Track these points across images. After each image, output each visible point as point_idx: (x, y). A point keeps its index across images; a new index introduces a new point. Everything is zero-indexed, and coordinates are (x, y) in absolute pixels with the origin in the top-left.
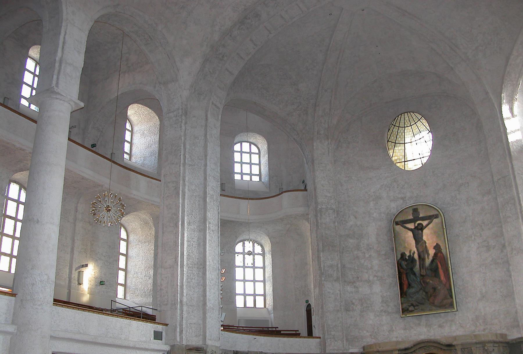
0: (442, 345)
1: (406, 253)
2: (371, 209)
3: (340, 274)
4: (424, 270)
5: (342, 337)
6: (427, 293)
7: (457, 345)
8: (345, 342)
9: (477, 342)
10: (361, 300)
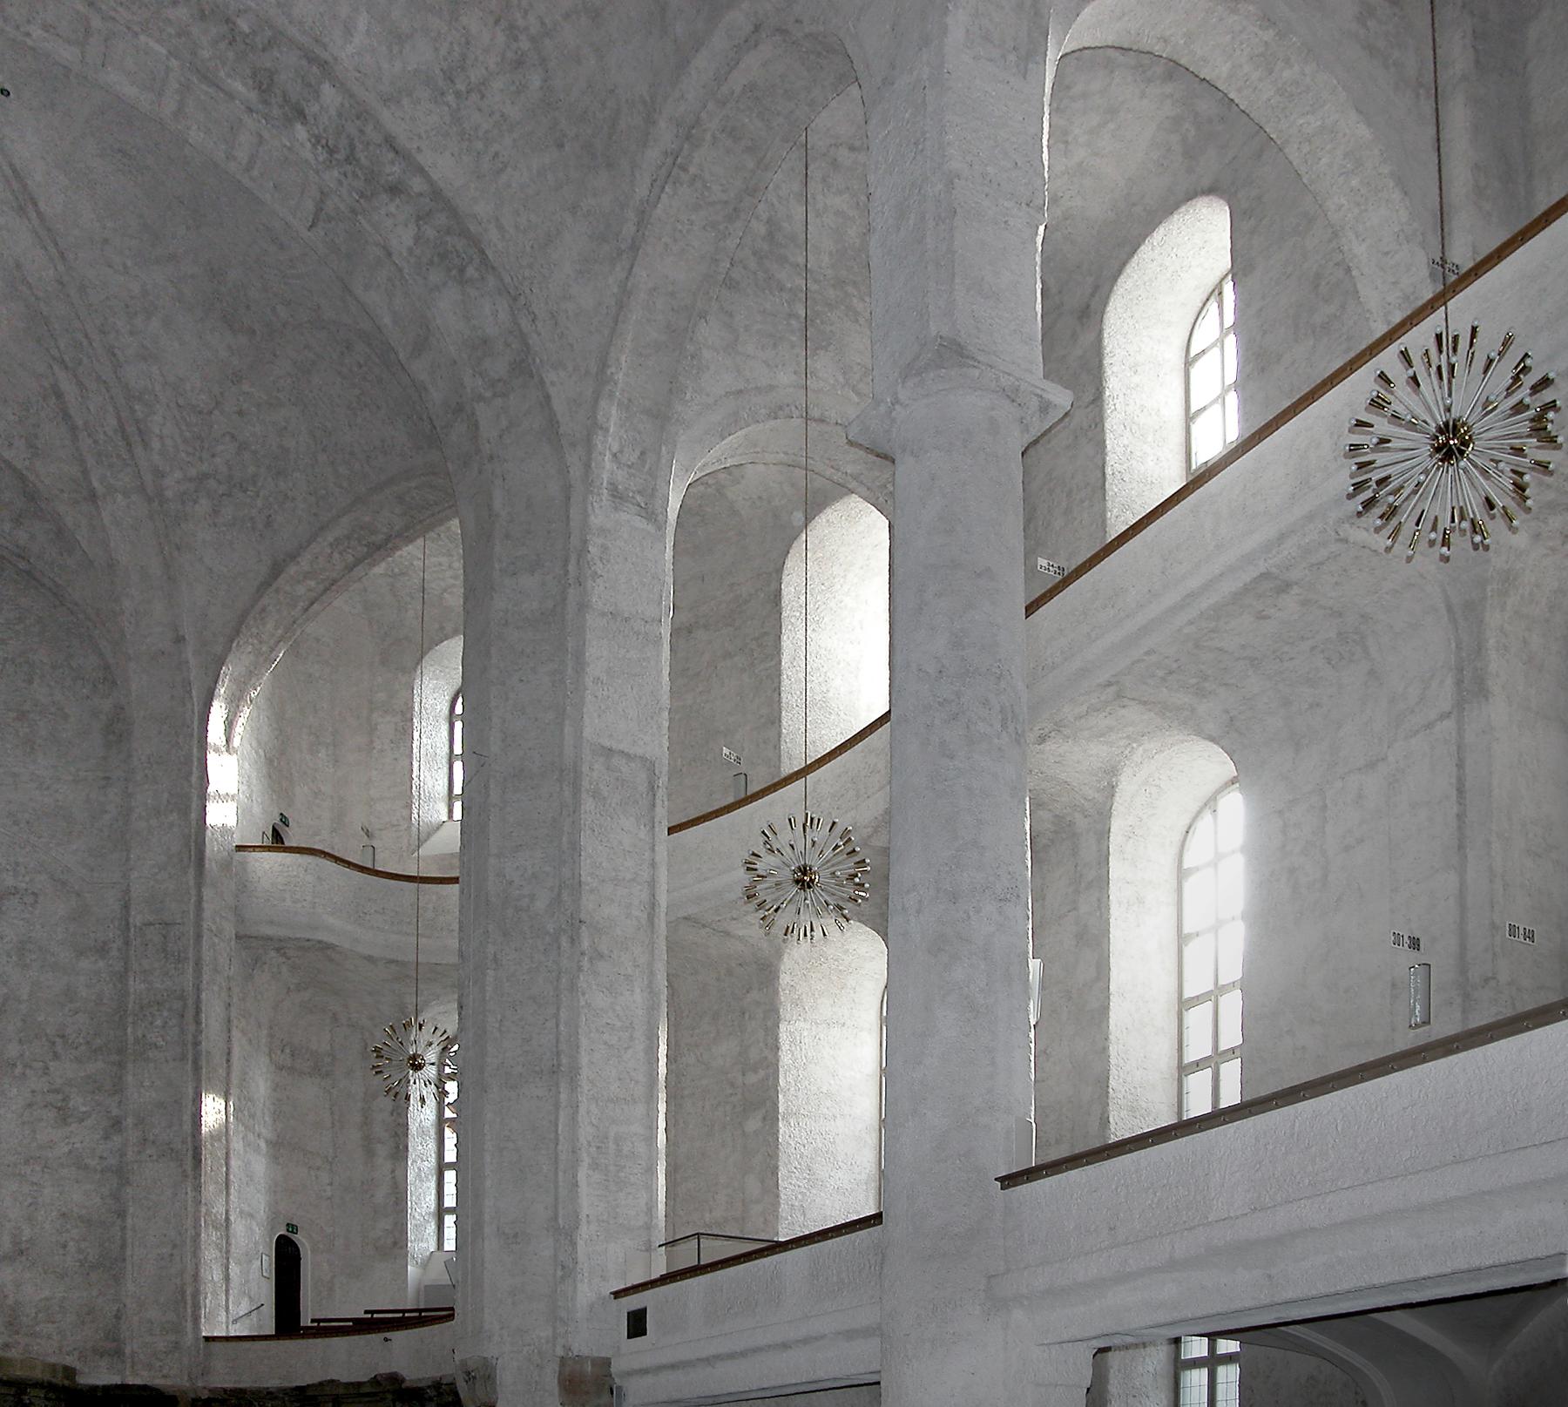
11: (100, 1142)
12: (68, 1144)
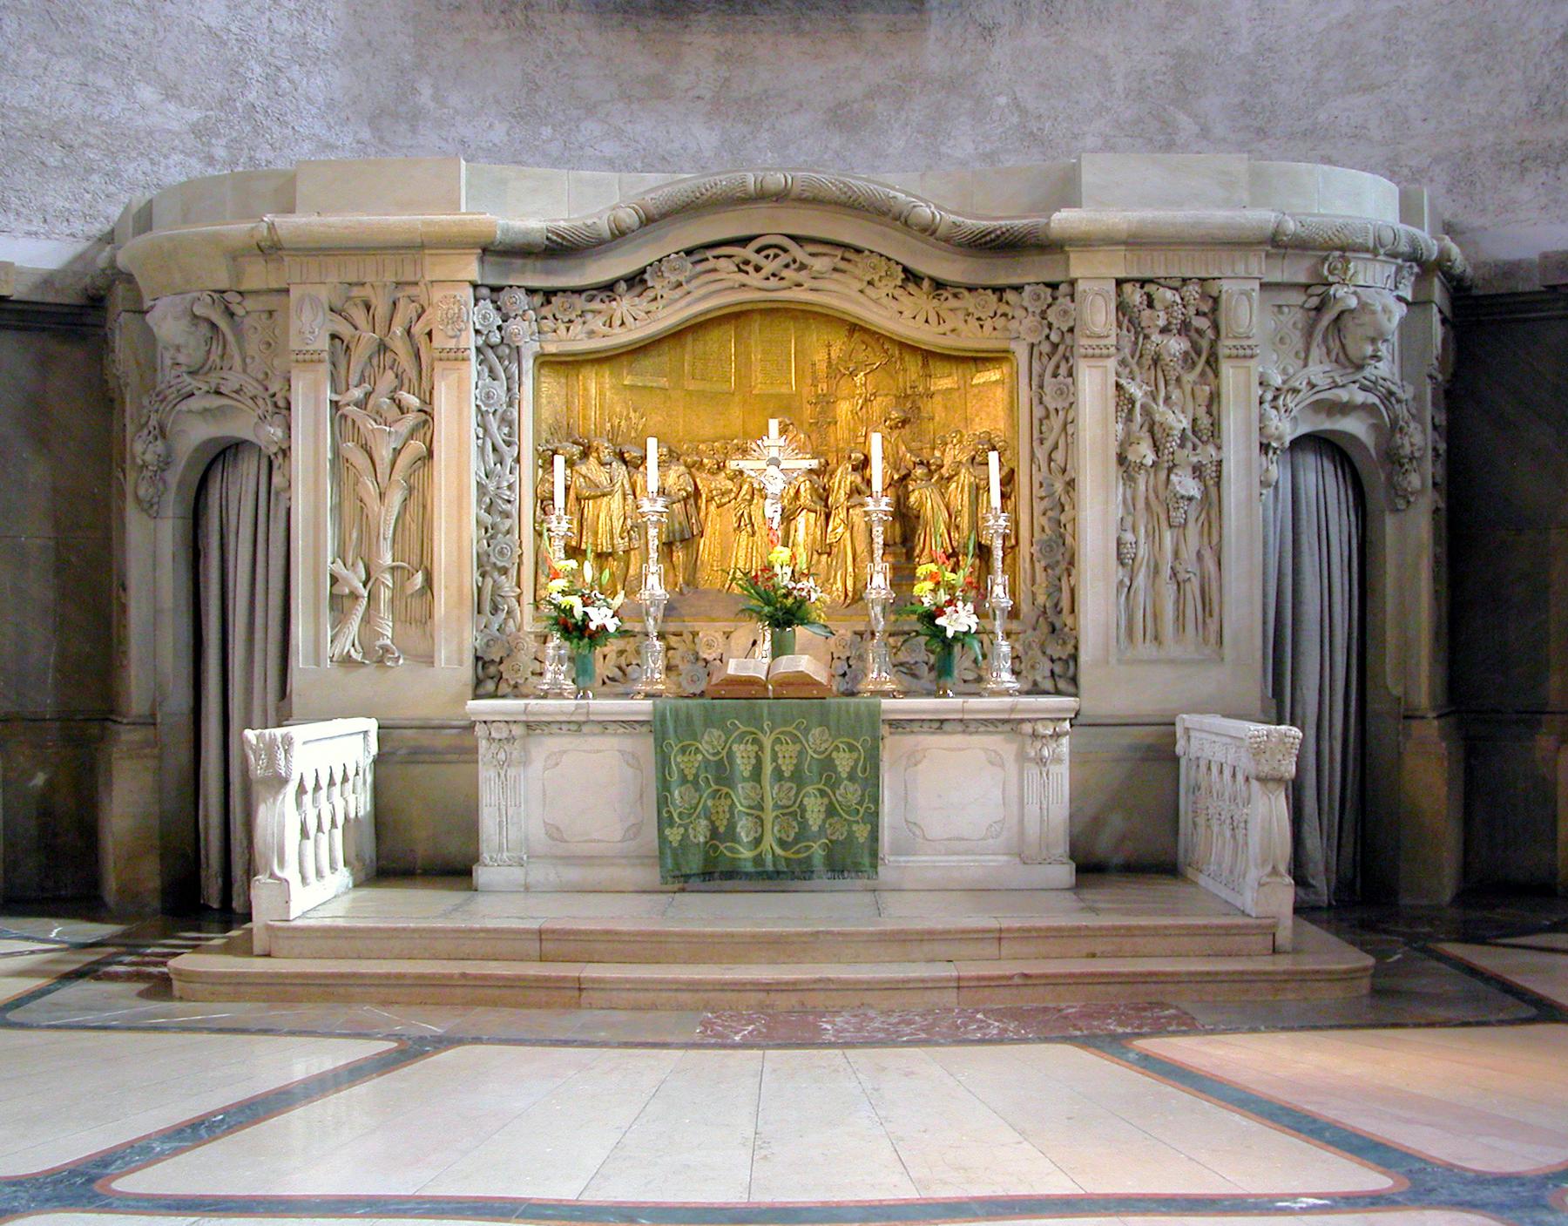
0: (928, 230)
7: (1087, 242)
9: (1291, 226)
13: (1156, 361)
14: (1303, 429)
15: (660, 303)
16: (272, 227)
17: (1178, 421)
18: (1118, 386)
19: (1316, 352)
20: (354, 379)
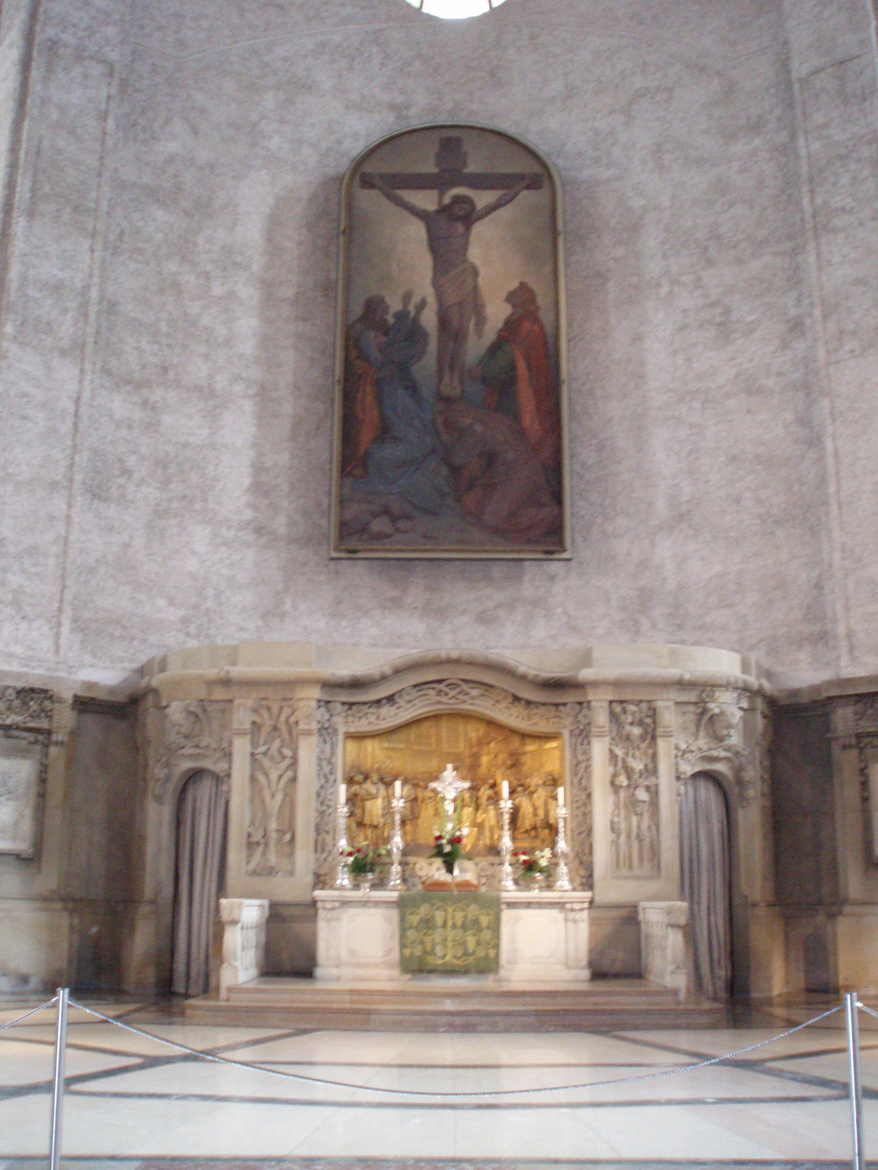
0: (523, 678)
1: (387, 298)
2: (264, 117)
3: (90, 330)
4: (456, 374)
5: (56, 605)
6: (455, 470)
7: (595, 684)
8: (65, 630)
9: (687, 677)
10: (162, 463)
11: (777, 354)
12: (734, 365)
13: (628, 738)
14: (696, 769)
15: (402, 709)
16: (228, 672)
17: (637, 766)
18: (611, 751)
19: (702, 733)
20: (261, 743)
